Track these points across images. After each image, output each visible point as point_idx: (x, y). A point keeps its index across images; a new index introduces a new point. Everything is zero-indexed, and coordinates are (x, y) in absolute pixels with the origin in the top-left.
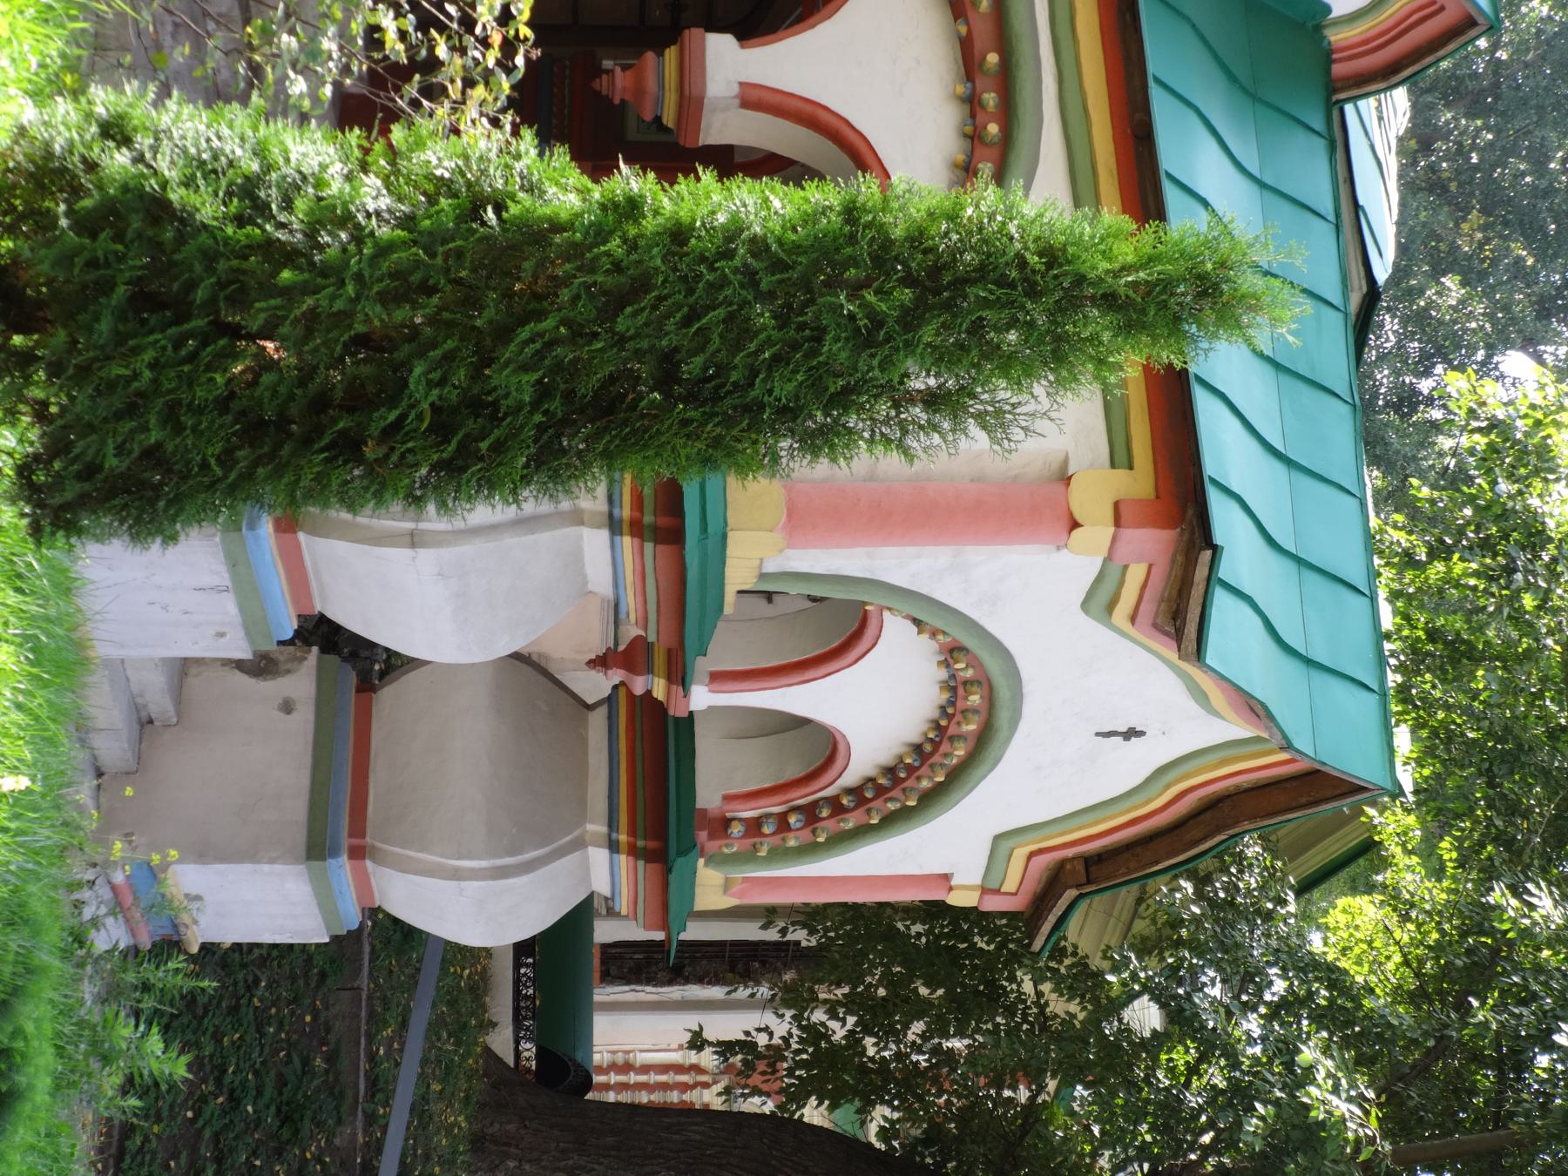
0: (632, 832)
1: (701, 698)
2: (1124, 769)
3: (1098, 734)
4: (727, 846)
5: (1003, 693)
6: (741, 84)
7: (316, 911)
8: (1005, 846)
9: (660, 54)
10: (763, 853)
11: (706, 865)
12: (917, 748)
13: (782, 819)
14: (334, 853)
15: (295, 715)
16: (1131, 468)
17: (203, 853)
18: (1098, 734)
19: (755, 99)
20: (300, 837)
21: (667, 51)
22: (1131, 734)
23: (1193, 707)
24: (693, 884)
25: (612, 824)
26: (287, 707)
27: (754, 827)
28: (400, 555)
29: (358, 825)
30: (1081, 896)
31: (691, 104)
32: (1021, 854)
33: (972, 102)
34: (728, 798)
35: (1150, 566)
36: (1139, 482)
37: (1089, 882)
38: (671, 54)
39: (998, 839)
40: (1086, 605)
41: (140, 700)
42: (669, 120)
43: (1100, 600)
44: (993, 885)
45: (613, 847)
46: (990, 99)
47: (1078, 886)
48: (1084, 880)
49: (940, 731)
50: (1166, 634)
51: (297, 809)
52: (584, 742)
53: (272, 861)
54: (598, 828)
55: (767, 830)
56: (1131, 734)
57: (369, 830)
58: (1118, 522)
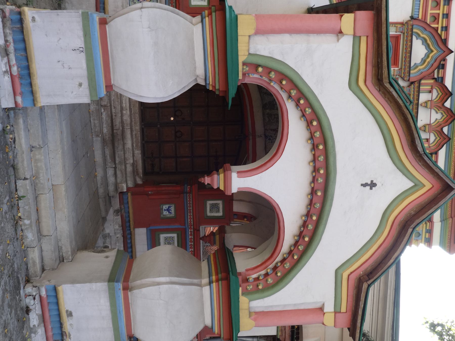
0: (217, 274)
4: (248, 286)
7: (111, 326)
8: (340, 272)
10: (260, 287)
11: (243, 294)
13: (267, 275)
14: (118, 281)
15: (109, 258)
17: (73, 282)
18: (362, 185)
20: (107, 278)
22: (372, 185)
24: (239, 302)
25: (210, 275)
26: (107, 257)
27: (257, 279)
28: (138, 12)
29: (127, 279)
30: (369, 286)
34: (247, 270)
35: (367, 37)
37: (370, 279)
41: (60, 245)
47: (367, 281)
48: (368, 279)
50: (377, 90)
51: (108, 273)
52: (201, 267)
53: (96, 282)
54: (205, 281)
55: (261, 278)
56: (372, 185)
57: (130, 281)
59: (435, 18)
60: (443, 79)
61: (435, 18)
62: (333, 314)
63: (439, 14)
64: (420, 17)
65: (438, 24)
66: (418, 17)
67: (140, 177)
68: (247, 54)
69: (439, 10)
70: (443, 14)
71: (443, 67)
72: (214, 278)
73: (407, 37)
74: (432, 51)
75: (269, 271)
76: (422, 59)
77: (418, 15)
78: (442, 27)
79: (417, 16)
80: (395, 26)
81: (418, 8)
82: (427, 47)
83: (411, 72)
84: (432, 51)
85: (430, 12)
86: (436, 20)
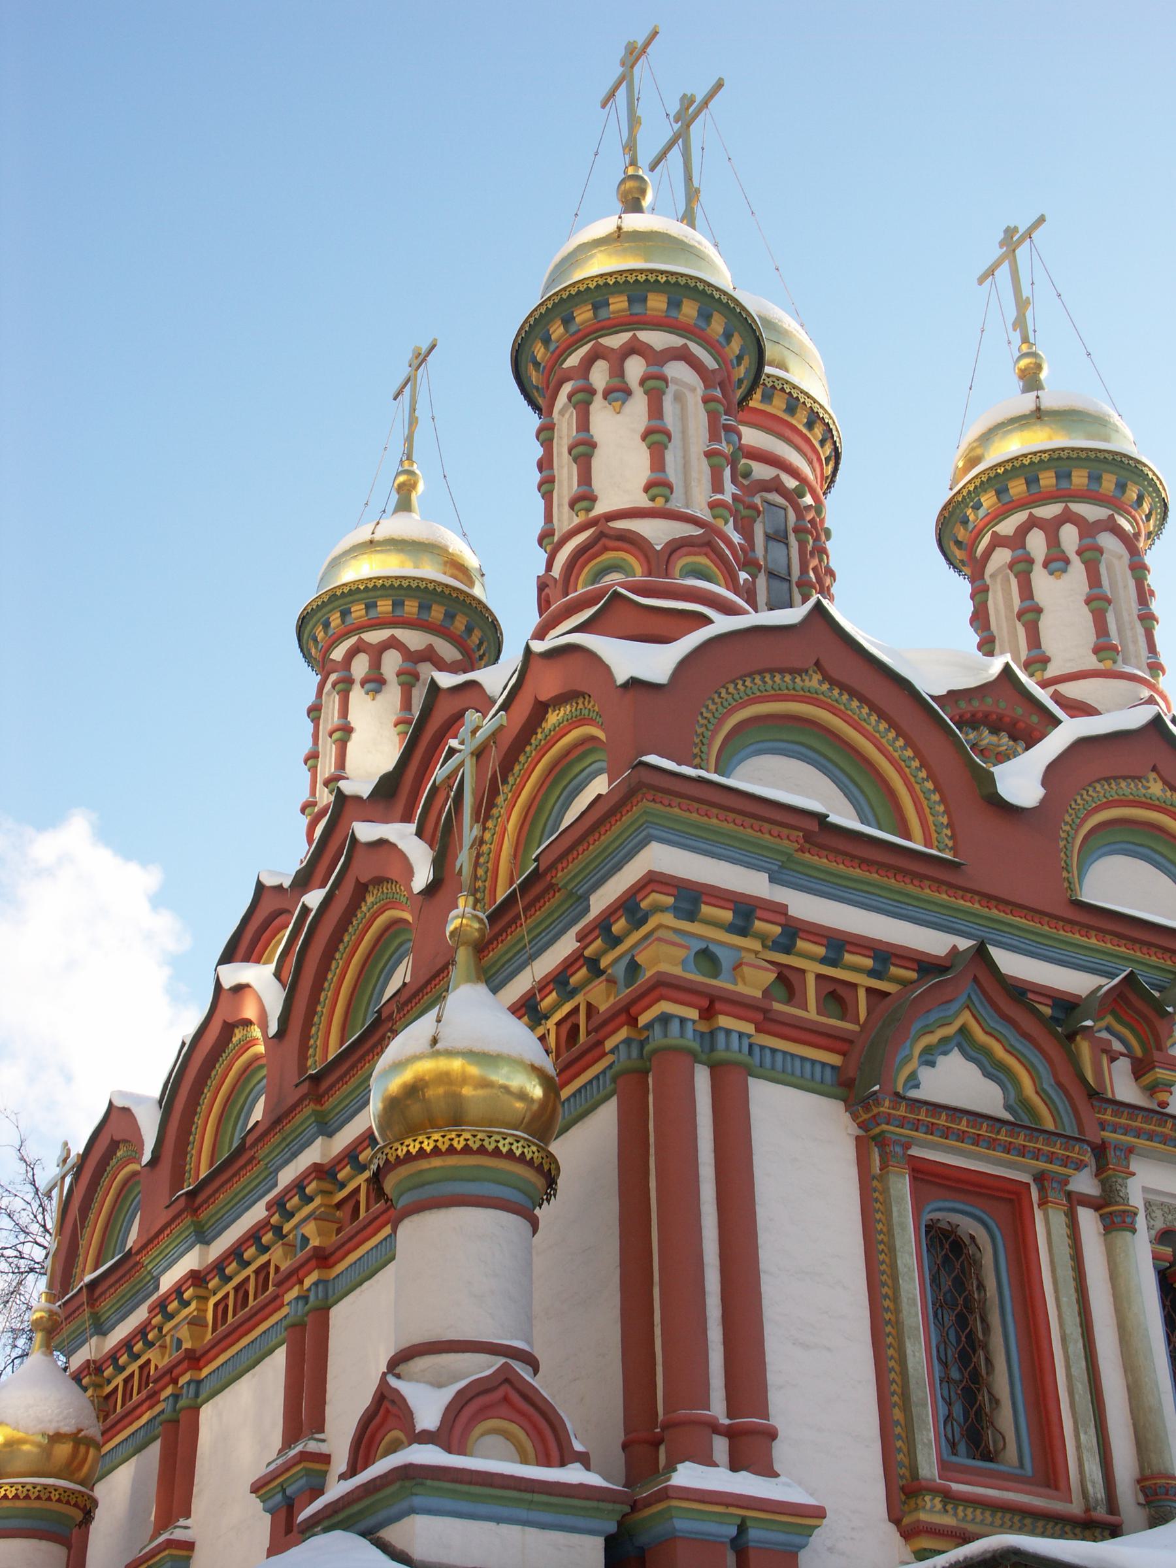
59: (836, 996)
60: (1067, 1005)
61: (836, 996)
63: (819, 977)
64: (835, 1059)
65: (854, 986)
66: (833, 1067)
69: (803, 971)
70: (823, 961)
71: (1019, 992)
73: (931, 1129)
74: (963, 1030)
76: (987, 1075)
77: (824, 1065)
78: (872, 973)
79: (828, 1072)
80: (880, 1178)
81: (798, 1063)
82: (943, 1047)
83: (1068, 1133)
84: (963, 1030)
85: (812, 1014)
86: (841, 991)
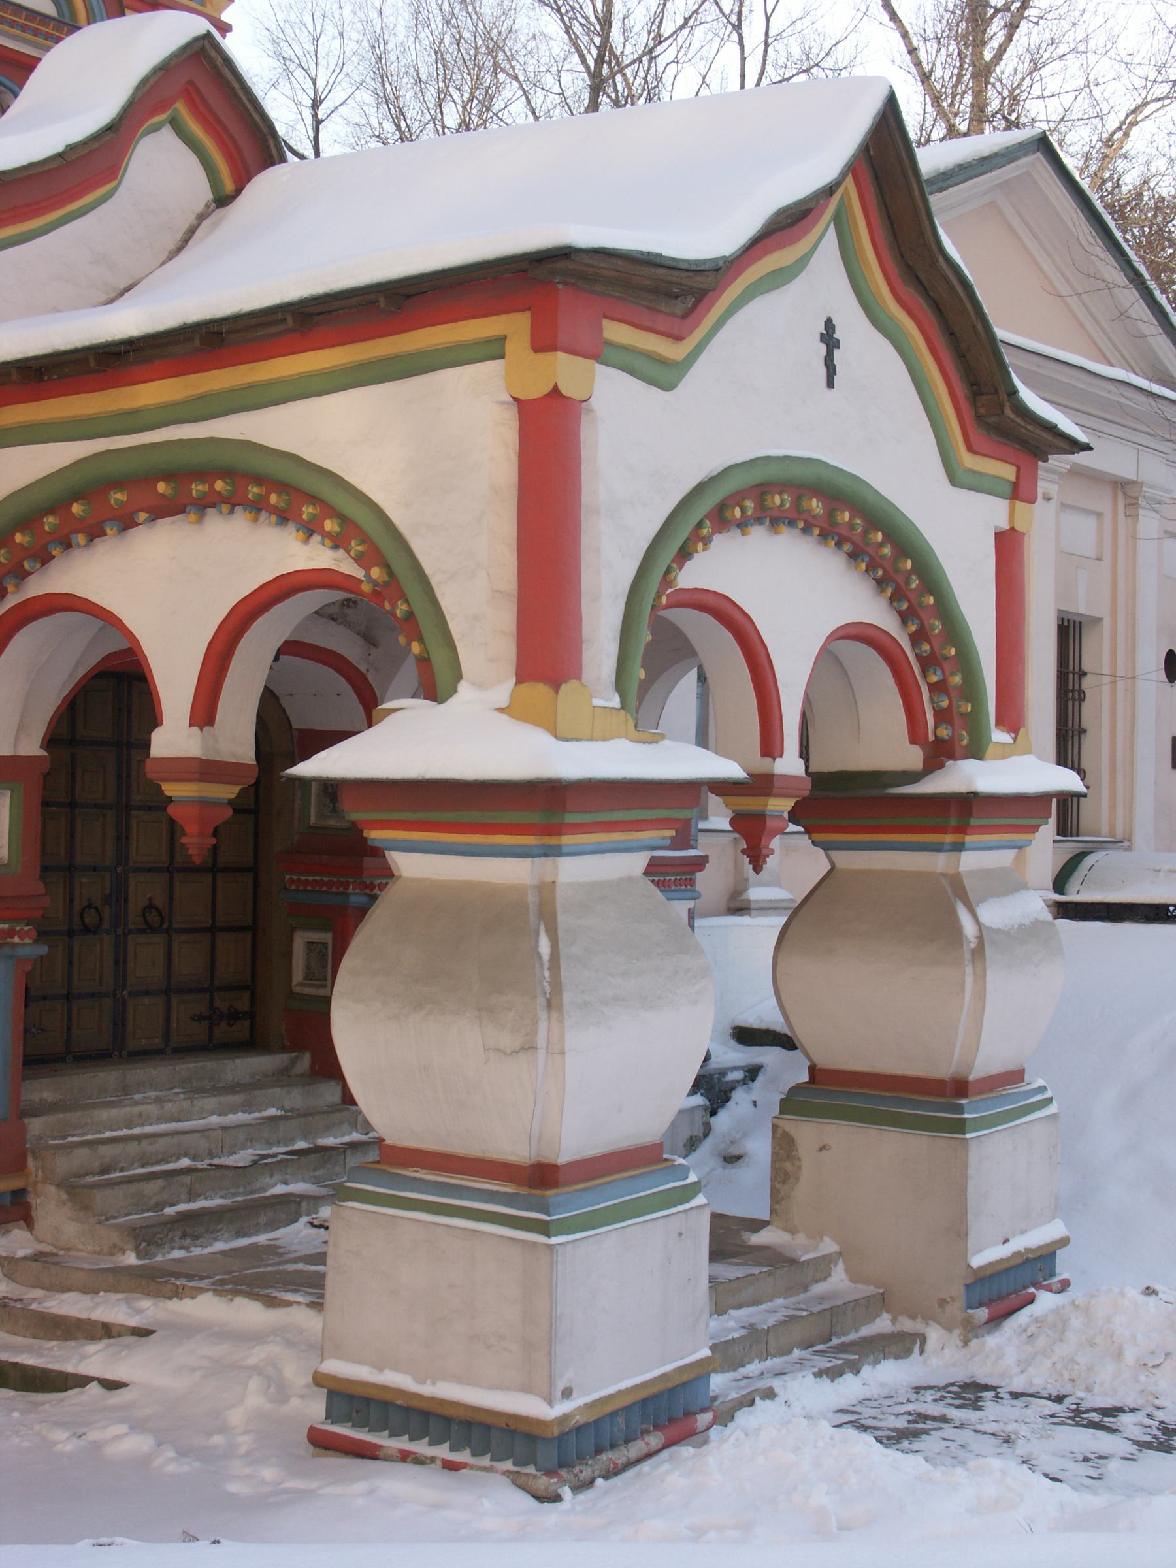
0: (942, 830)
1: (790, 764)
2: (870, 354)
3: (830, 384)
5: (773, 472)
6: (191, 725)
9: (170, 800)
12: (853, 556)
16: (505, 338)
19: (204, 712)
21: (167, 793)
23: (796, 288)
25: (937, 848)
31: (207, 770)
32: (970, 461)
33: (204, 505)
34: (914, 738)
35: (605, 316)
36: (515, 326)
38: (171, 789)
39: (954, 481)
40: (668, 387)
42: (229, 792)
43: (663, 375)
44: (1008, 489)
45: (959, 847)
46: (198, 489)
49: (827, 532)
51: (917, 1143)
58: (552, 348)
62: (1018, 503)
67: (294, 1061)
68: (622, 712)
72: (948, 838)
75: (934, 679)
